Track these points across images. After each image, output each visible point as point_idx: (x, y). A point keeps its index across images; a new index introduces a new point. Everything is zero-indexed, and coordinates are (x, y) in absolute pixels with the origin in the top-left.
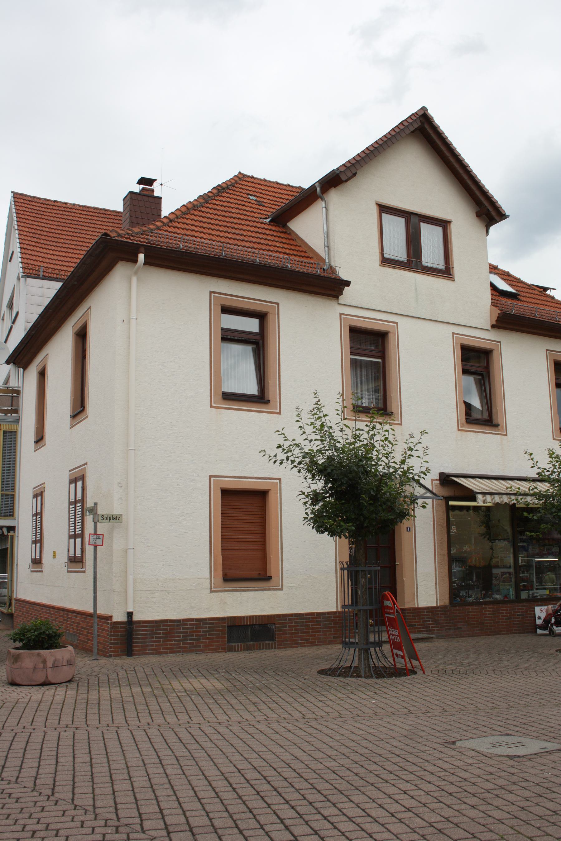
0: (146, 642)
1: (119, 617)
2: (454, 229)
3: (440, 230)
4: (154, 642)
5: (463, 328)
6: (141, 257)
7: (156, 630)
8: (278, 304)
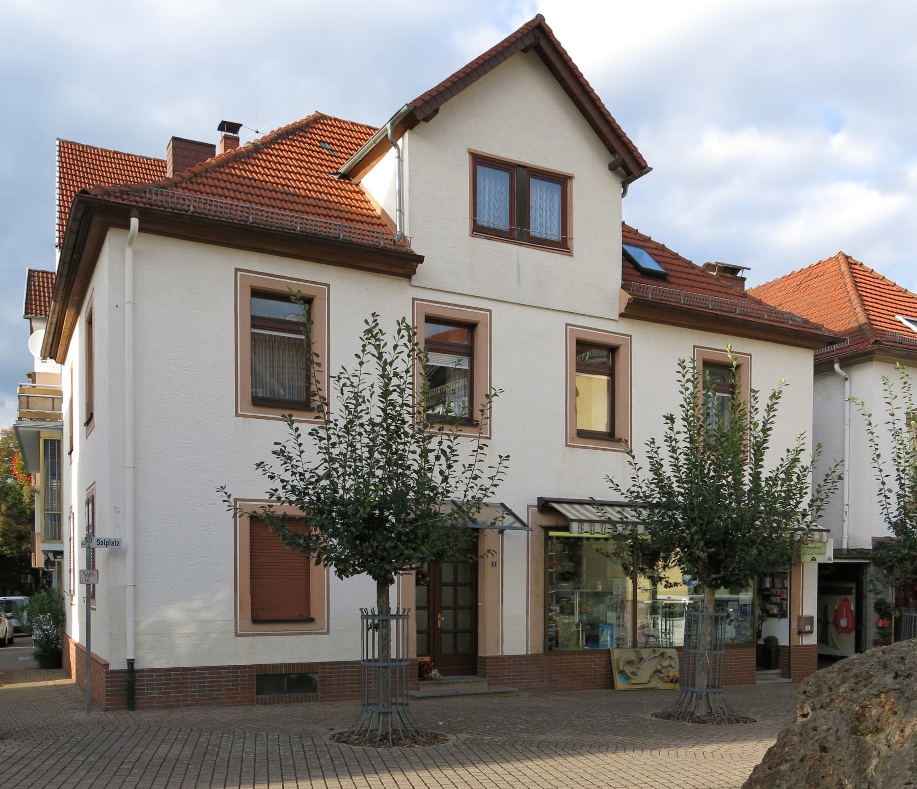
0: (152, 694)
1: (117, 664)
2: (577, 188)
3: (557, 188)
4: (163, 693)
5: (479, 300)
6: (134, 222)
7: (166, 680)
8: (328, 286)
